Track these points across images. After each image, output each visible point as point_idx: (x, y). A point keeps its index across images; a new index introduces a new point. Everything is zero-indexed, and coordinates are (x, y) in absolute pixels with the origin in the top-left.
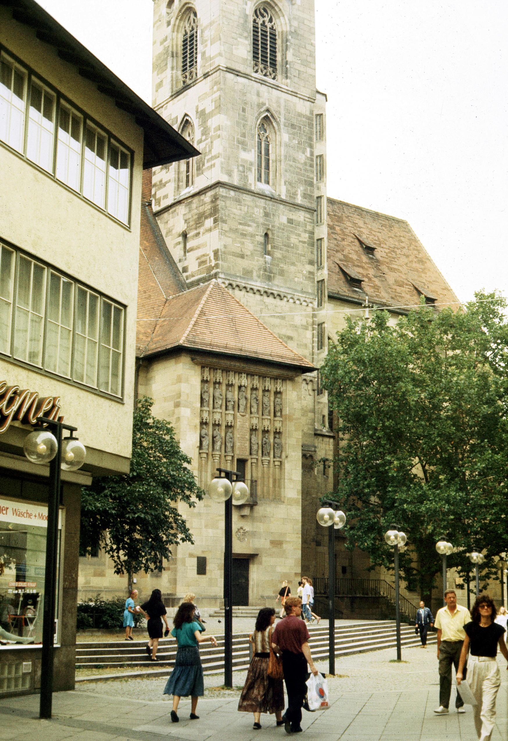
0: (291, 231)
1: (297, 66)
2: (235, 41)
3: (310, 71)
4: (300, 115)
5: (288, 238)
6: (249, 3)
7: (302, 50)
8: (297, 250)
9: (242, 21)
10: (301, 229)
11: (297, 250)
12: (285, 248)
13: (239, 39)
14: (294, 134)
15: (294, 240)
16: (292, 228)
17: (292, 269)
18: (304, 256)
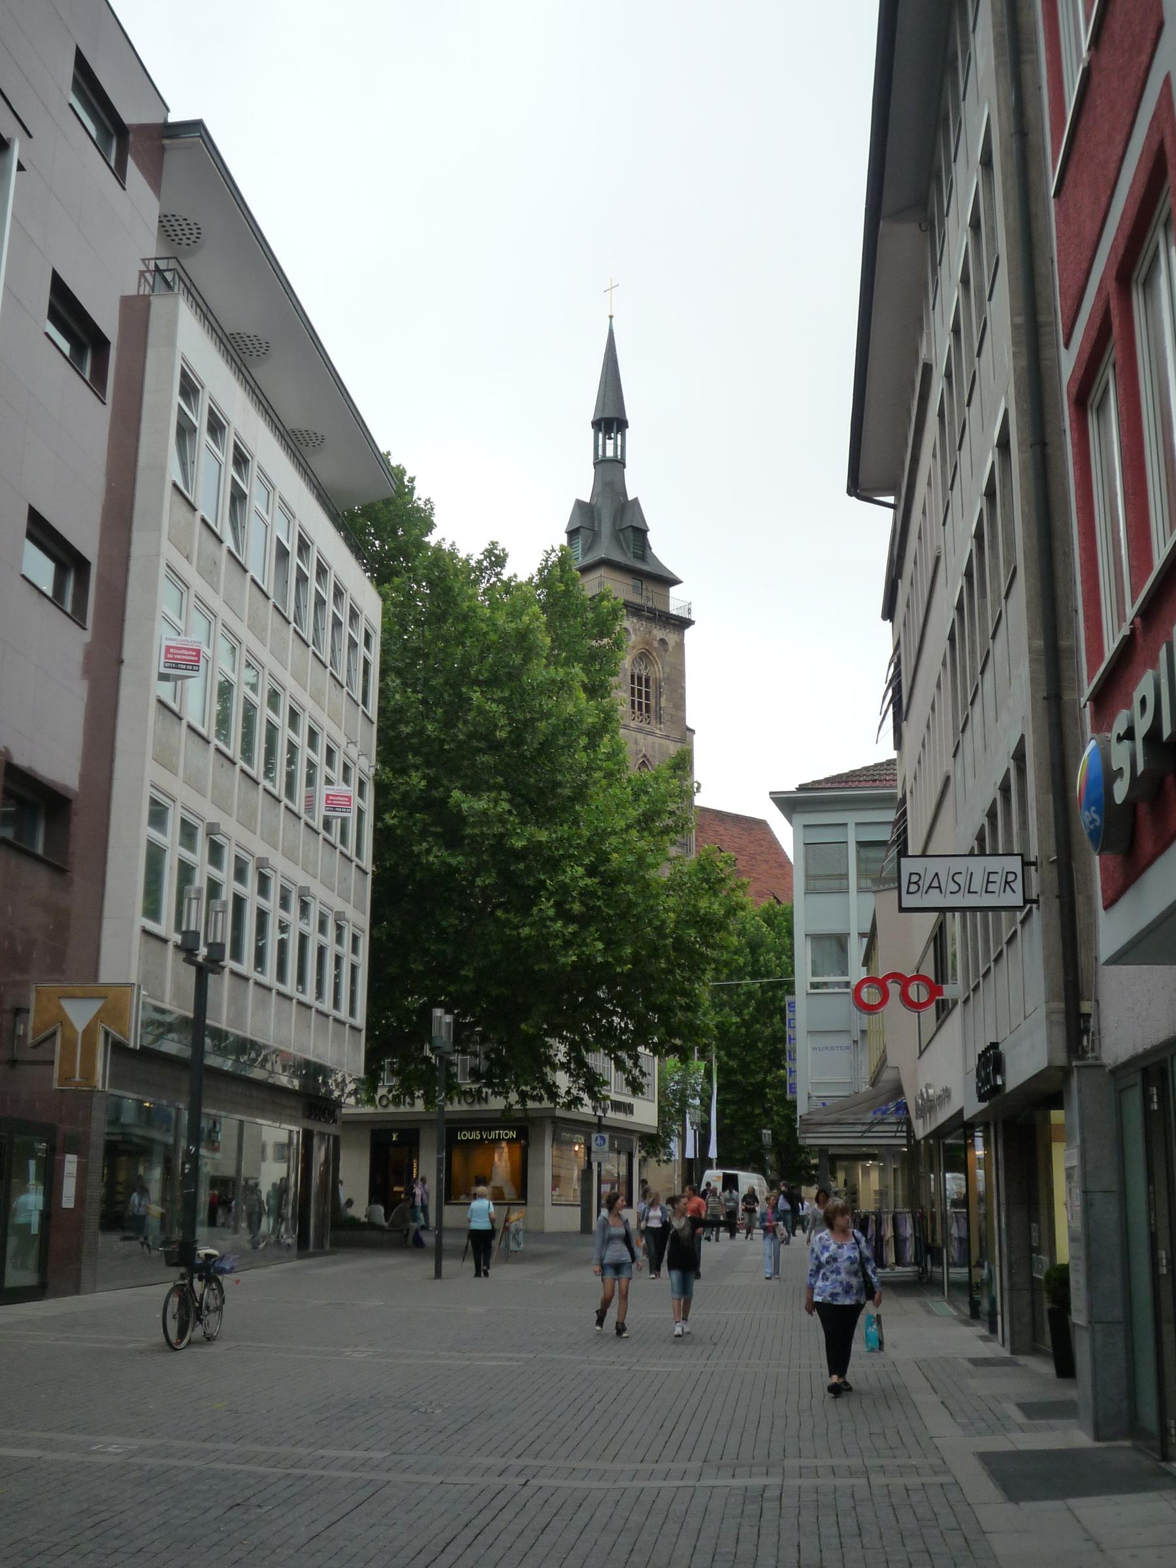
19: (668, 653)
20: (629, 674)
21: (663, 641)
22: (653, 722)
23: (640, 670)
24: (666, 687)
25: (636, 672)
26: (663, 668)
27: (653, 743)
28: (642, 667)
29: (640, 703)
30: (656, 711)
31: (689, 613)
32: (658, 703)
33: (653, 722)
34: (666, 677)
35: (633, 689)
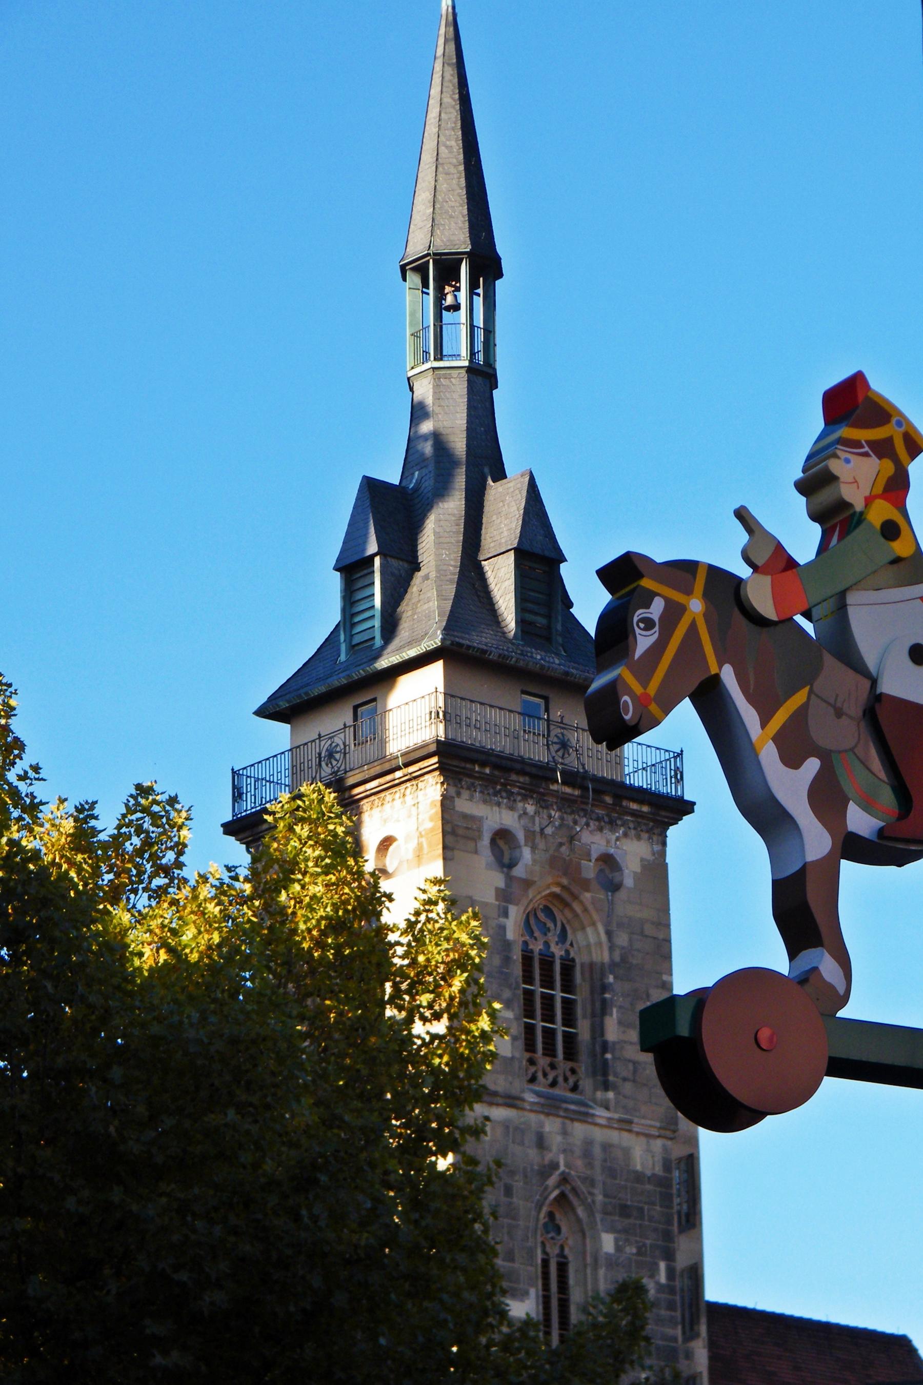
4: (639, 1177)
6: (513, 910)
14: (625, 1231)
19: (622, 895)
20: (517, 955)
21: (608, 861)
22: (587, 1084)
23: (547, 944)
25: (537, 947)
26: (609, 934)
28: (553, 938)
29: (549, 1035)
30: (593, 1055)
32: (598, 1030)
33: (587, 1084)
34: (617, 959)
35: (529, 995)
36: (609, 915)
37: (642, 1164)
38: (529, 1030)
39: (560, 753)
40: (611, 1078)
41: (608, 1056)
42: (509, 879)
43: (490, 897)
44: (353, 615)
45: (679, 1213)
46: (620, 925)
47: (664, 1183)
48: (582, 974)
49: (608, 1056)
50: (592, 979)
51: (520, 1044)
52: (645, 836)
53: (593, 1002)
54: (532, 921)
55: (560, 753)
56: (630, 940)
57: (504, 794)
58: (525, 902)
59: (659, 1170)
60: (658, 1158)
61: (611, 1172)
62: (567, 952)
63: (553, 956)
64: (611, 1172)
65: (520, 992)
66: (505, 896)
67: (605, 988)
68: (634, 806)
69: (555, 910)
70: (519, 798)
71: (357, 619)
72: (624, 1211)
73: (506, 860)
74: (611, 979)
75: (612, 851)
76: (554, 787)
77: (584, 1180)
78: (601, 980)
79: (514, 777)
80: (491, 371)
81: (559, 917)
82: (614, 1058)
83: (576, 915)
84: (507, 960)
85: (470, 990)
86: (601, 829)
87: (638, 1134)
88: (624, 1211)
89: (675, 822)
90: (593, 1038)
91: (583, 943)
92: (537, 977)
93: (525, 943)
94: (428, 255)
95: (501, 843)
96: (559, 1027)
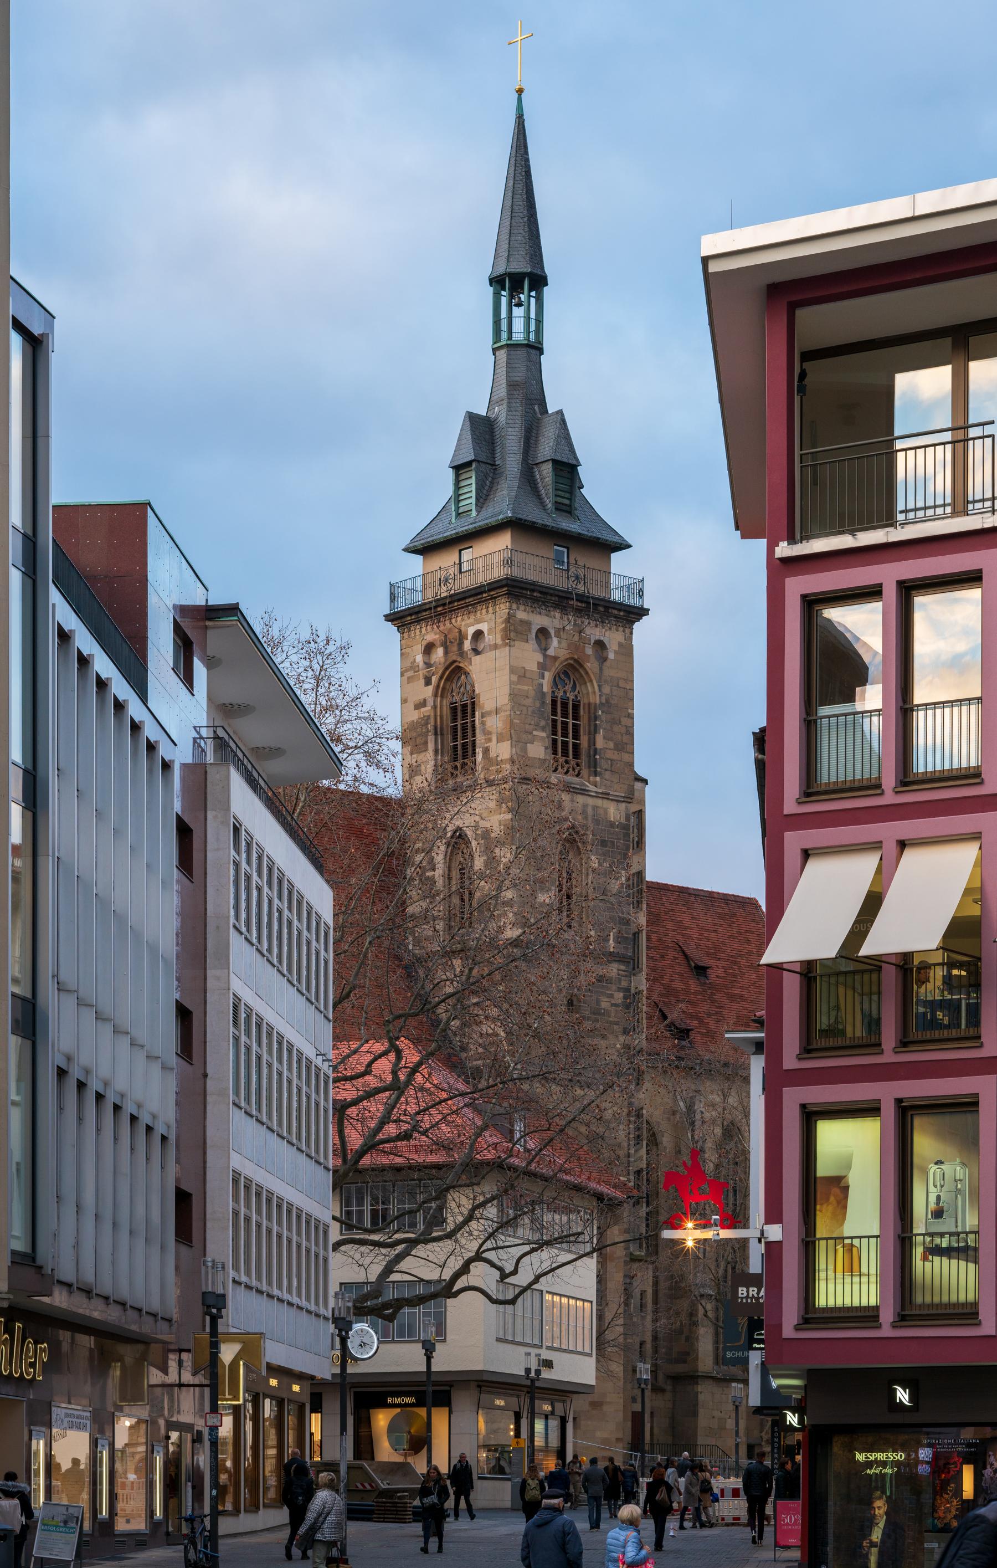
0: (602, 992)
1: (609, 754)
2: (530, 736)
3: (626, 757)
4: (612, 824)
5: (598, 1002)
6: (547, 674)
7: (616, 728)
8: (609, 1017)
9: (538, 704)
10: (614, 987)
11: (609, 1017)
12: (593, 1016)
13: (535, 733)
14: (604, 855)
15: (605, 1004)
16: (603, 987)
17: (603, 1043)
18: (617, 1023)
19: (607, 664)
20: (548, 700)
21: (600, 645)
22: (585, 772)
23: (565, 692)
24: (603, 717)
25: (560, 694)
26: (600, 686)
27: (585, 806)
28: (568, 688)
29: (565, 744)
30: (589, 756)
31: (641, 594)
32: (592, 742)
33: (585, 772)
34: (604, 701)
35: (554, 721)
36: (600, 677)
37: (614, 817)
38: (554, 742)
39: (575, 583)
40: (598, 769)
41: (597, 757)
42: (545, 656)
43: (534, 667)
44: (459, 495)
45: (633, 841)
46: (606, 681)
47: (625, 827)
48: (584, 709)
49: (597, 757)
50: (589, 712)
51: (550, 751)
52: (621, 629)
53: (589, 725)
54: (557, 679)
55: (575, 583)
56: (611, 690)
57: (543, 607)
58: (553, 670)
59: (623, 820)
60: (623, 814)
61: (597, 822)
62: (576, 697)
63: (568, 699)
64: (597, 822)
65: (550, 722)
66: (542, 667)
67: (596, 718)
68: (615, 612)
69: (570, 673)
70: (552, 609)
71: (461, 498)
72: (603, 843)
73: (543, 646)
74: (600, 713)
75: (602, 638)
76: (571, 602)
77: (582, 826)
78: (595, 713)
79: (549, 597)
80: (540, 346)
81: (572, 677)
82: (601, 758)
83: (582, 676)
84: (543, 703)
85: (555, 916)
86: (596, 626)
87: (612, 800)
88: (603, 843)
89: (638, 620)
90: (589, 746)
91: (585, 692)
92: (559, 712)
93: (553, 692)
94: (505, 274)
95: (540, 635)
96: (570, 740)
